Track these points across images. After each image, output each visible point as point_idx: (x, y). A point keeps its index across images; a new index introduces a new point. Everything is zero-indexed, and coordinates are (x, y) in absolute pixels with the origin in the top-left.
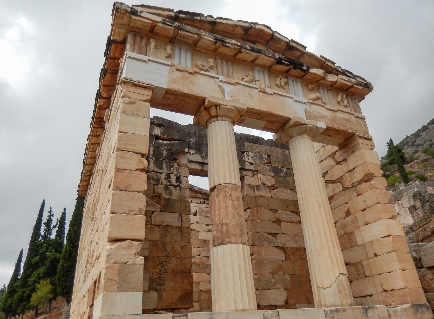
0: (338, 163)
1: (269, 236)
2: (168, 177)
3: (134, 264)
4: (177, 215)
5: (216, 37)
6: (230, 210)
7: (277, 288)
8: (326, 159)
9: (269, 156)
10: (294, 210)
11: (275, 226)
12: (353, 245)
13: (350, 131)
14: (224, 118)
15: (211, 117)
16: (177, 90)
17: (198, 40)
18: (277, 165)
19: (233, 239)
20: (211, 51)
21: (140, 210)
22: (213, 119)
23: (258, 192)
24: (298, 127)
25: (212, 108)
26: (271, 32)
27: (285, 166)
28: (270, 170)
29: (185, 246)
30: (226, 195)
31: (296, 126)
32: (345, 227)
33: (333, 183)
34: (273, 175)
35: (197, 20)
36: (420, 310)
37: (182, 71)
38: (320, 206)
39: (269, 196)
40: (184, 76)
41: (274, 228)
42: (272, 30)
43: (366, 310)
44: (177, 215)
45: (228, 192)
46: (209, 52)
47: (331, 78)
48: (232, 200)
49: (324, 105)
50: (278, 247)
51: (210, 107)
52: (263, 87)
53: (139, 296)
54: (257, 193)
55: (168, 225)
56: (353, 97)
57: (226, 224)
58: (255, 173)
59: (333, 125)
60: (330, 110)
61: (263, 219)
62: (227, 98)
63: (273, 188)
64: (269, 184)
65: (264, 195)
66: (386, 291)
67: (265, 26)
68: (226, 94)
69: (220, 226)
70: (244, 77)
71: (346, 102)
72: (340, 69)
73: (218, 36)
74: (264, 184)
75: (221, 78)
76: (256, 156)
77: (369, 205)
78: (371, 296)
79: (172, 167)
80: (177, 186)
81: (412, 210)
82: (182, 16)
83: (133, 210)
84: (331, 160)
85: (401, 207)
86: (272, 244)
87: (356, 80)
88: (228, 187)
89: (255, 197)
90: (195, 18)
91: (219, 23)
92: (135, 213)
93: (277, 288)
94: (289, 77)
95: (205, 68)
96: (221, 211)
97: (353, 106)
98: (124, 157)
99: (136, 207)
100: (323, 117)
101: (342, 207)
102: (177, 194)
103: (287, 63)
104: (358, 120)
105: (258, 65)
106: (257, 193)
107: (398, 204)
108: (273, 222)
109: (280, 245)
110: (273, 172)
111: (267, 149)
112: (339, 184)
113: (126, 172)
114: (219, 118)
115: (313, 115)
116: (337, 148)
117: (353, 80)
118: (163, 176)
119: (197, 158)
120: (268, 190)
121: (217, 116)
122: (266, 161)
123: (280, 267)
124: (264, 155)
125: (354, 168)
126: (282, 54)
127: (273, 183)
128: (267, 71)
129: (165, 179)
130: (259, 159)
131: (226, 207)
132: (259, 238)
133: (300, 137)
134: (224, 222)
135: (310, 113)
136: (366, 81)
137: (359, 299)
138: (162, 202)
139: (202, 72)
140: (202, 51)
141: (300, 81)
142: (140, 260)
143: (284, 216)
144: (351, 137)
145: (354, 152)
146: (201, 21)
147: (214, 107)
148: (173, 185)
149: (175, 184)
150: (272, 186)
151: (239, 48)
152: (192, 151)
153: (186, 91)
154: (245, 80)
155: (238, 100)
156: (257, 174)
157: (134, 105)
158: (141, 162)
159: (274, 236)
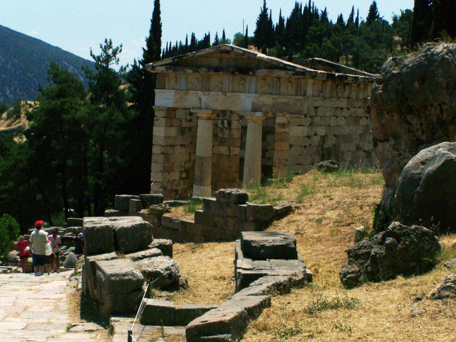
2: (223, 123)
4: (226, 148)
26: (231, 49)
29: (231, 166)
44: (226, 148)
54: (283, 130)
55: (221, 154)
60: (273, 98)
68: (202, 103)
79: (226, 115)
80: (228, 128)
89: (281, 133)
100: (265, 105)
102: (227, 133)
106: (283, 130)
117: (290, 72)
118: (220, 122)
129: (221, 124)
132: (279, 163)
138: (218, 140)
148: (225, 128)
149: (227, 127)
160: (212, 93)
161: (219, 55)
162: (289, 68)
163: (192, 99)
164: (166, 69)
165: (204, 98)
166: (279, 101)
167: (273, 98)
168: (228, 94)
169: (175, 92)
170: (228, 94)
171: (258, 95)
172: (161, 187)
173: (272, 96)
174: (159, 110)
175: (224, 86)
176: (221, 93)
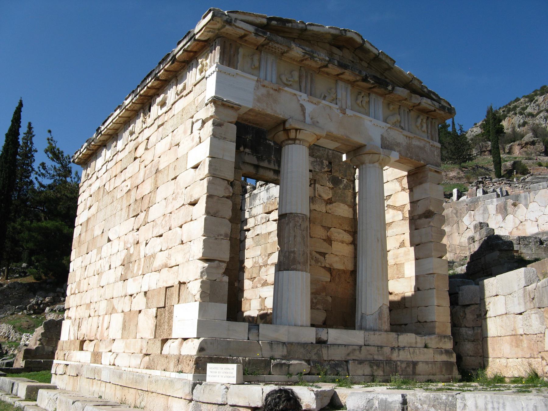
0: (403, 189)
1: (318, 256)
3: (221, 281)
5: (305, 50)
6: (299, 239)
7: (318, 309)
8: (392, 181)
9: (330, 163)
10: (347, 229)
11: (326, 245)
12: (400, 276)
13: (422, 162)
14: (301, 143)
15: (289, 139)
16: (260, 110)
17: (287, 52)
18: (336, 174)
19: (299, 267)
20: (296, 61)
21: (226, 235)
22: (290, 142)
23: (313, 204)
24: (371, 155)
25: (292, 131)
26: (361, 42)
27: (346, 176)
28: (329, 180)
30: (296, 225)
31: (370, 154)
32: (397, 258)
33: (395, 209)
34: (331, 186)
35: (288, 28)
36: (443, 340)
37: (267, 87)
38: (378, 240)
39: (324, 211)
40: (269, 95)
41: (323, 247)
42: (362, 39)
43: (398, 335)
45: (298, 222)
46: (295, 63)
47: (416, 99)
48: (301, 230)
49: (402, 130)
50: (325, 267)
51: (290, 130)
52: (344, 107)
53: (224, 307)
56: (434, 121)
57: (294, 252)
58: (312, 182)
59: (407, 154)
61: (314, 236)
62: (308, 119)
63: (329, 202)
64: (326, 197)
65: (318, 209)
66: (420, 322)
67: (356, 33)
68: (307, 115)
69: (287, 253)
70: (326, 95)
71: (425, 125)
72: (425, 90)
73: (307, 49)
74: (320, 196)
75: (304, 96)
76: (317, 161)
77: (423, 240)
78: (406, 325)
81: (471, 241)
82: (274, 23)
83: (221, 235)
84: (398, 184)
85: (473, 219)
86: (319, 264)
87: (440, 103)
88: (299, 216)
90: (287, 25)
91: (310, 30)
92: (222, 237)
93: (318, 309)
94: (371, 94)
95: (290, 83)
96: (291, 239)
97: (431, 132)
98: (213, 183)
99: (223, 232)
100: (398, 145)
101: (398, 237)
103: (372, 82)
104: (433, 149)
105: (341, 79)
107: (470, 216)
108: (324, 240)
109: (328, 266)
110: (332, 183)
111: (329, 154)
112: (400, 212)
113: (216, 198)
114: (297, 142)
115: (388, 141)
116: (406, 173)
119: (253, 160)
120: (324, 204)
121: (295, 140)
122: (326, 169)
123: (324, 288)
124: (324, 161)
125: (418, 201)
126: (368, 64)
127: (330, 196)
128: (349, 85)
130: (319, 165)
131: (295, 236)
133: (371, 165)
134: (292, 250)
135: (386, 138)
136: (450, 105)
137: (395, 326)
139: (286, 89)
140: (288, 61)
141: (382, 100)
142: (226, 279)
143: (336, 234)
144: (421, 167)
145: (421, 183)
146: (291, 28)
147: (294, 131)
150: (329, 199)
151: (327, 63)
152: (247, 150)
153: (269, 111)
154: (327, 99)
155: (318, 122)
156: (315, 184)
157: (223, 127)
158: (228, 188)
159: (322, 256)
160: (323, 102)
161: (328, 46)
162: (434, 97)
163: (289, 104)
164: (256, 30)
165: (309, 108)
166: (414, 143)
167: (406, 137)
168: (349, 112)
169: (257, 81)
170: (349, 112)
171: (389, 126)
172: (225, 273)
173: (406, 133)
174: (223, 105)
175: (339, 97)
176: (337, 107)
